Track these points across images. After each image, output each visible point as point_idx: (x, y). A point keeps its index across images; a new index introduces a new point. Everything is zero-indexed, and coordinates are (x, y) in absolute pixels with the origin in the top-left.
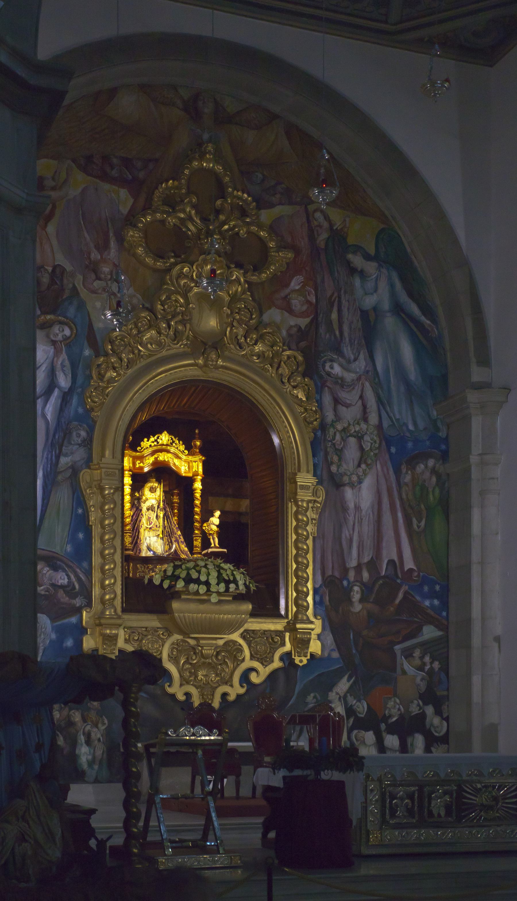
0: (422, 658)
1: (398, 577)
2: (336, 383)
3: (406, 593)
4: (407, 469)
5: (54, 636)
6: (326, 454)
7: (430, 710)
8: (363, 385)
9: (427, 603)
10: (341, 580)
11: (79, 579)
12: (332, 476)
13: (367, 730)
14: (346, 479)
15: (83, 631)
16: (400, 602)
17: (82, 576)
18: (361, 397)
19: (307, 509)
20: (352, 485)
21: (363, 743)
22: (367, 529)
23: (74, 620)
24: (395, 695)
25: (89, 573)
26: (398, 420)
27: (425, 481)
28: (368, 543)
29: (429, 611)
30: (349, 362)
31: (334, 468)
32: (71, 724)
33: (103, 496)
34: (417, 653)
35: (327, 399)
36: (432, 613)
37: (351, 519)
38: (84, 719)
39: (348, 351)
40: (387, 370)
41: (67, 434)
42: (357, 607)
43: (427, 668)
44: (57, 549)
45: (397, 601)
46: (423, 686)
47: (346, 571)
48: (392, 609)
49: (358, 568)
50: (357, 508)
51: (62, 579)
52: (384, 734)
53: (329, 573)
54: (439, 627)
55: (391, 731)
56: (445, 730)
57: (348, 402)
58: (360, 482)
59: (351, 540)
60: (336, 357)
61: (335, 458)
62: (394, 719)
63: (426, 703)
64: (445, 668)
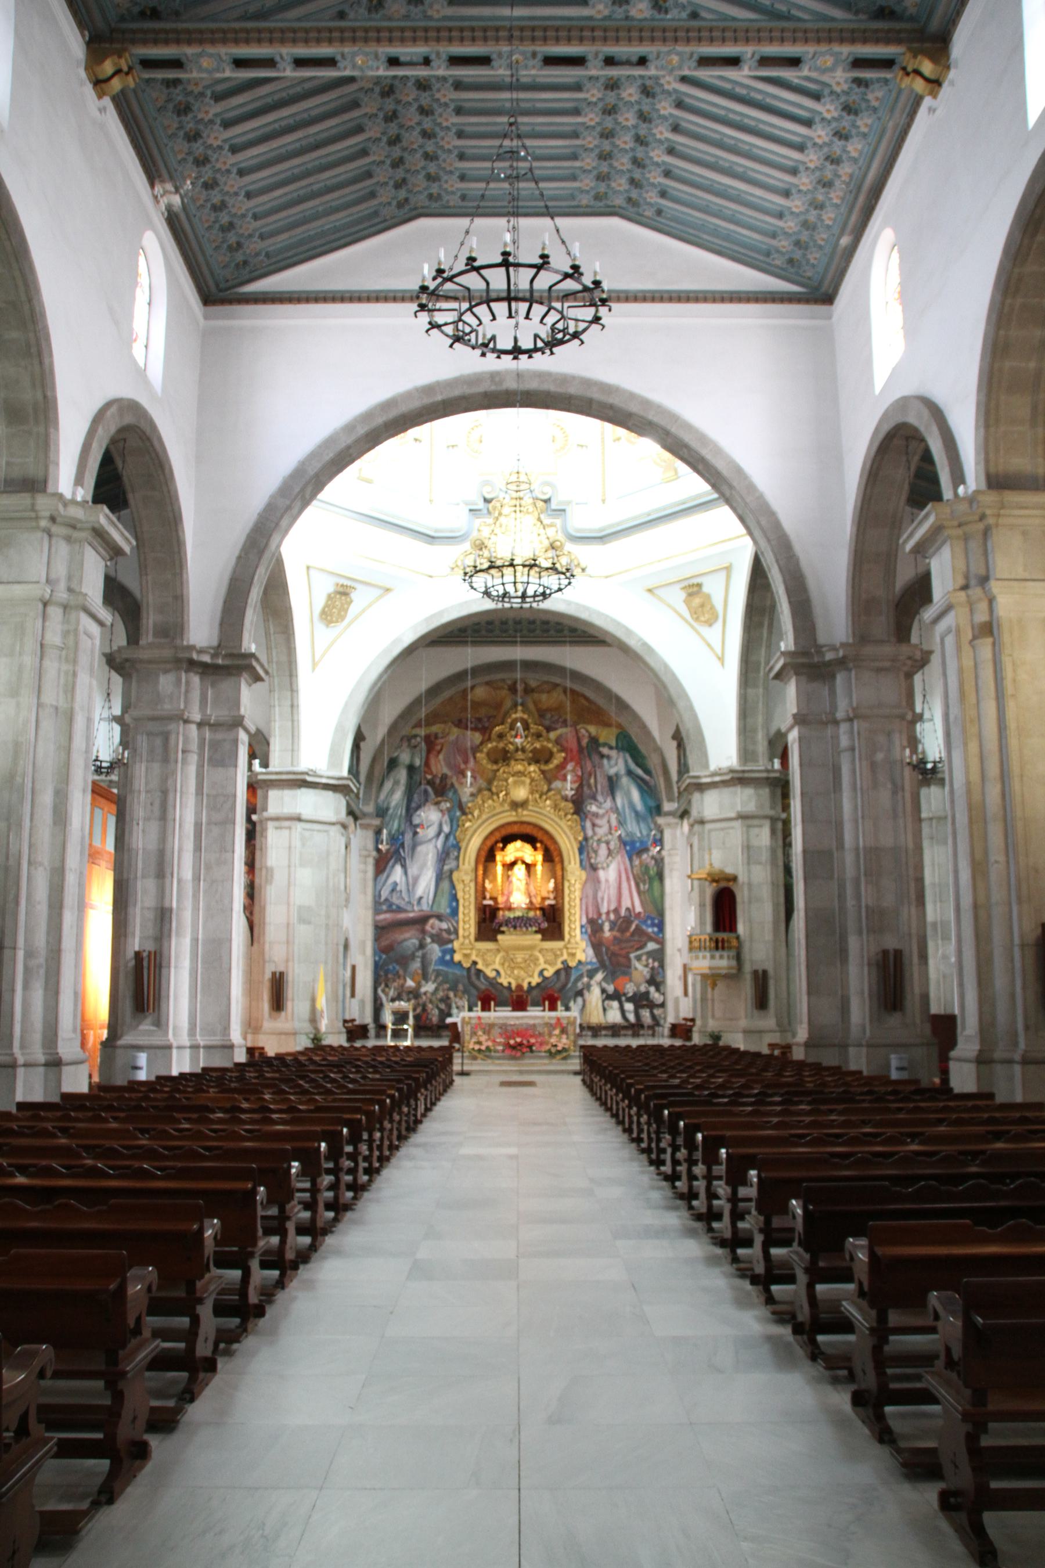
0: (647, 960)
3: (637, 926)
5: (440, 954)
6: (588, 853)
7: (652, 989)
9: (650, 930)
14: (600, 866)
15: (454, 951)
18: (609, 822)
20: (603, 869)
21: (611, 1007)
22: (613, 892)
23: (450, 946)
24: (631, 980)
25: (457, 922)
28: (614, 899)
31: (593, 861)
32: (448, 998)
34: (644, 958)
35: (588, 824)
37: (603, 885)
38: (455, 996)
39: (600, 798)
42: (607, 934)
46: (648, 976)
47: (600, 915)
48: (628, 934)
49: (608, 913)
50: (607, 881)
53: (590, 916)
55: (629, 1000)
58: (608, 866)
59: (603, 899)
61: (593, 855)
64: (662, 966)
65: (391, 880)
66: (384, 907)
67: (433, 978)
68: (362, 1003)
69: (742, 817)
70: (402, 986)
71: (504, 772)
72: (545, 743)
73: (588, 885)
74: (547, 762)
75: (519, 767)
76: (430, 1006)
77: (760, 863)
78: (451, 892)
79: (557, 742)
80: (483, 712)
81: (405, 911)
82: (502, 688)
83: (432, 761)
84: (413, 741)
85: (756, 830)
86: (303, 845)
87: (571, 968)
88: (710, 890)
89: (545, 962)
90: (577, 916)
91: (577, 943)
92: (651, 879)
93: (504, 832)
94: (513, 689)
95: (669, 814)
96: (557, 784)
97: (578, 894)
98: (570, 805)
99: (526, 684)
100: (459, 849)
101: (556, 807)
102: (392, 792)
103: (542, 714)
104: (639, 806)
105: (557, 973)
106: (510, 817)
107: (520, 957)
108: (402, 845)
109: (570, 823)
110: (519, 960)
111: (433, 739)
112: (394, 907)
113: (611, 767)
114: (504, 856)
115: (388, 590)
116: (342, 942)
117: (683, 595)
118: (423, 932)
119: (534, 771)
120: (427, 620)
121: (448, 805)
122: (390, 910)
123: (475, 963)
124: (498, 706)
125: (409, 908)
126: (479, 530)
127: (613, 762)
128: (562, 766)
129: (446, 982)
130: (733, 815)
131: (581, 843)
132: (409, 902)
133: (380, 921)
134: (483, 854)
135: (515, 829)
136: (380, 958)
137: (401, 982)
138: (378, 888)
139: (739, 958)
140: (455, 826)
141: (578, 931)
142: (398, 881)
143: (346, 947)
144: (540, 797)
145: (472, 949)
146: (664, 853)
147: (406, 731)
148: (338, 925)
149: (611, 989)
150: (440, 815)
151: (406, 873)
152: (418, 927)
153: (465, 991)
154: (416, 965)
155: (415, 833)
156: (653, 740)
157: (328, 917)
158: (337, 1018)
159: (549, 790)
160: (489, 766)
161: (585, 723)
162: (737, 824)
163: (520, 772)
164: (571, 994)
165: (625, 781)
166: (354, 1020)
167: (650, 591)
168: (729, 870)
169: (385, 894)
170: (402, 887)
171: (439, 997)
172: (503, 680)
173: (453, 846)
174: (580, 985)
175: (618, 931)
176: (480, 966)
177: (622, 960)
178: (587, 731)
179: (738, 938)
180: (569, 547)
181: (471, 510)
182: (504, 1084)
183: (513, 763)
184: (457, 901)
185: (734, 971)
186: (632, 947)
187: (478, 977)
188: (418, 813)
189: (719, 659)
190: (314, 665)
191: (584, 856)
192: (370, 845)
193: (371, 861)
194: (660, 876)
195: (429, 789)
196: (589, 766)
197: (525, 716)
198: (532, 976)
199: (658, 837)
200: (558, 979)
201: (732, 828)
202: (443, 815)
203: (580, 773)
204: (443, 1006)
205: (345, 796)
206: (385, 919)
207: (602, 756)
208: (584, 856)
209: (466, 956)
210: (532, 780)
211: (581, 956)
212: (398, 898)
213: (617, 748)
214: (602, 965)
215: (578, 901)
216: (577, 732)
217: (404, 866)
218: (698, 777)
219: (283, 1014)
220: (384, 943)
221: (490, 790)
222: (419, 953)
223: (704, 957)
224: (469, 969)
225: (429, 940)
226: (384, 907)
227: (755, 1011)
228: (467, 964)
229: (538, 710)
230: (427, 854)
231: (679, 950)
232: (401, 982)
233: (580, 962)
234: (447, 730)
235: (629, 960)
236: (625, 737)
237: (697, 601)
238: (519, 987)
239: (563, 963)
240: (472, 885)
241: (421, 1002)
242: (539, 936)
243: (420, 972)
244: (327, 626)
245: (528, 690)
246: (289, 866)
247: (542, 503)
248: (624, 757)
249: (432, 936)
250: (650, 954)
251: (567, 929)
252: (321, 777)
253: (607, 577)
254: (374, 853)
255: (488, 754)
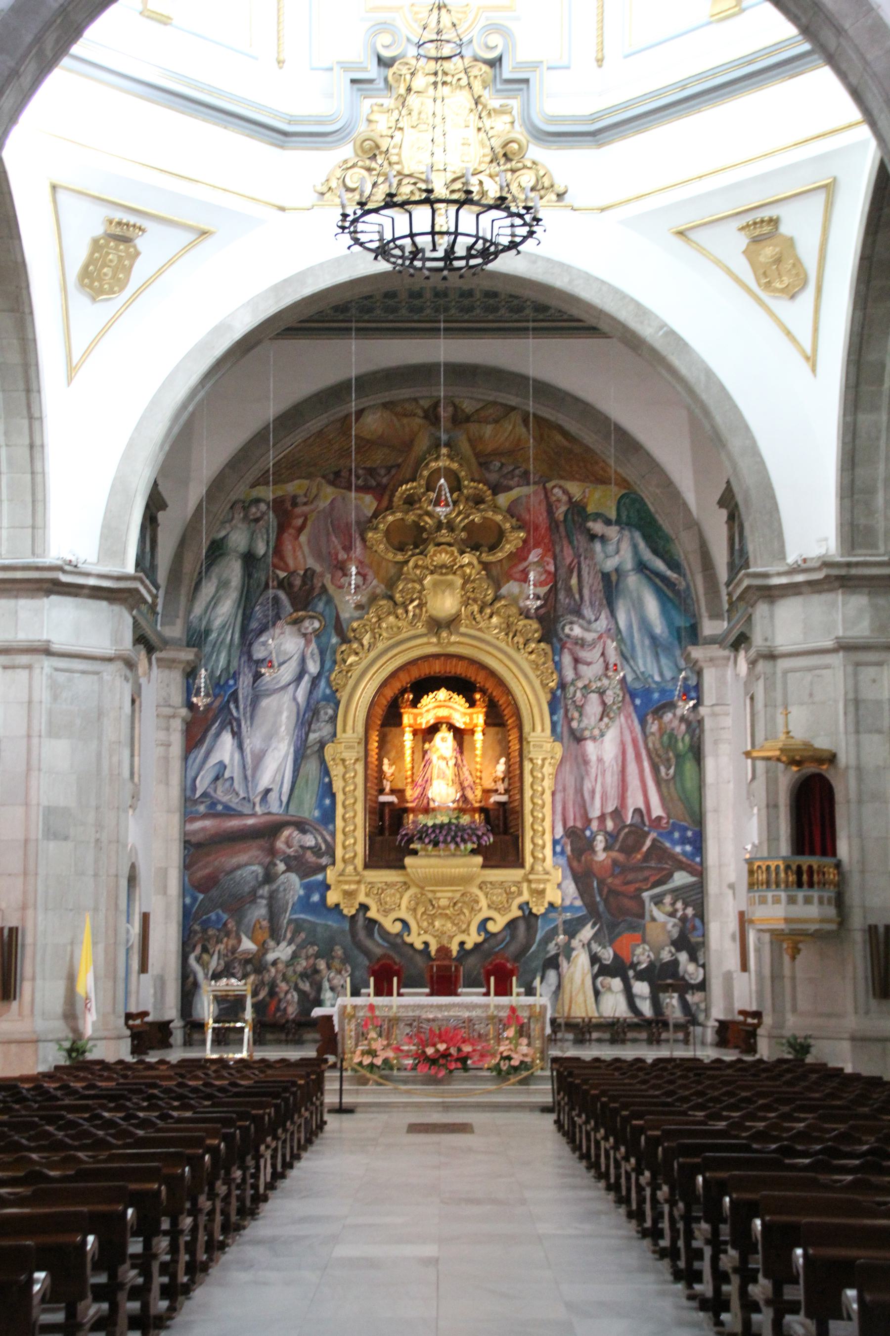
0: (673, 904)
1: (645, 825)
2: (576, 644)
3: (654, 840)
4: (654, 720)
5: (302, 892)
7: (683, 957)
8: (605, 643)
9: (678, 849)
10: (583, 831)
11: (325, 841)
12: (572, 732)
13: (613, 976)
14: (587, 734)
15: (328, 887)
16: (649, 849)
17: (329, 838)
18: (603, 654)
19: (543, 766)
20: (594, 739)
21: (609, 989)
22: (611, 780)
23: (320, 877)
24: (644, 941)
25: (333, 834)
26: (643, 673)
27: (673, 729)
29: (681, 858)
30: (589, 622)
31: (574, 724)
32: (316, 971)
33: (345, 767)
34: (668, 900)
35: (567, 660)
36: (684, 859)
37: (593, 771)
38: (329, 967)
39: (588, 612)
40: (630, 627)
41: (316, 713)
42: (601, 856)
43: (679, 914)
44: (306, 815)
45: (645, 848)
46: (675, 934)
47: (588, 821)
48: (639, 856)
49: (602, 818)
50: (600, 760)
51: (309, 840)
52: (632, 981)
53: (571, 823)
54: (692, 873)
55: (641, 976)
56: (701, 977)
57: (589, 660)
58: (602, 735)
59: (593, 792)
60: (575, 619)
61: (576, 715)
62: (644, 966)
63: (679, 950)
64: (701, 915)
65: (213, 760)
66: (202, 808)
67: (289, 935)
68: (160, 982)
69: (844, 647)
70: (234, 950)
71: (416, 566)
72: (490, 514)
73: (567, 767)
74: (492, 548)
75: (444, 558)
76: (283, 986)
77: (879, 731)
78: (321, 780)
79: (511, 512)
80: (378, 458)
81: (240, 815)
82: (415, 415)
83: (288, 547)
84: (254, 510)
85: (871, 671)
86: (55, 698)
87: (536, 916)
88: (786, 779)
89: (489, 907)
90: (547, 824)
91: (547, 873)
92: (678, 756)
93: (416, 673)
94: (432, 416)
95: (713, 640)
96: (511, 588)
97: (548, 784)
98: (535, 625)
99: (454, 406)
100: (337, 704)
101: (508, 628)
102: (215, 601)
103: (483, 461)
104: (659, 627)
105: (512, 924)
106: (428, 646)
107: (444, 897)
108: (234, 697)
109: (533, 656)
110: (443, 902)
111: (288, 505)
112: (220, 807)
113: (607, 557)
114: (416, 716)
115: (204, 233)
116: (125, 871)
117: (742, 241)
118: (272, 852)
119: (469, 564)
120: (276, 289)
121: (317, 624)
122: (212, 814)
123: (364, 908)
124: (408, 445)
125: (247, 811)
126: (370, 121)
127: (611, 548)
128: (520, 555)
129: (313, 944)
130: (829, 644)
131: (553, 692)
132: (246, 799)
133: (195, 832)
134: (380, 712)
135: (437, 668)
136: (195, 899)
137: (232, 942)
138: (191, 773)
139: (840, 902)
140: (328, 665)
141: (548, 851)
142: (227, 761)
143: (132, 880)
144: (481, 611)
145: (359, 882)
146: (703, 710)
147: (241, 491)
148: (118, 841)
149: (607, 955)
150: (302, 642)
151: (240, 747)
152: (262, 842)
153: (347, 959)
154: (259, 912)
155: (258, 676)
156: (685, 504)
157: (99, 826)
158: (114, 1012)
159: (497, 598)
160: (390, 556)
161: (562, 478)
162: (837, 660)
163: (443, 566)
164: (538, 963)
165: (633, 581)
166: (145, 1014)
167: (681, 233)
168: (822, 743)
169: (202, 785)
170: (233, 771)
171: (299, 969)
172: (416, 400)
173: (326, 698)
174: (552, 949)
175: (621, 850)
176: (372, 914)
177: (628, 903)
178: (565, 492)
179: (838, 865)
180: (535, 152)
181: (353, 81)
182: (414, 1128)
183: (432, 549)
184: (333, 796)
185: (833, 927)
186: (646, 879)
187: (370, 934)
188: (262, 639)
189: (807, 359)
190: (72, 371)
191: (560, 715)
192: (177, 697)
193: (177, 725)
194: (697, 753)
195: (282, 595)
196: (568, 555)
197: (455, 466)
198: (466, 931)
199: (693, 682)
200: (513, 937)
201: (827, 667)
202: (308, 643)
203: (552, 568)
204: (306, 986)
205: (131, 609)
206: (203, 829)
207: (593, 537)
208: (560, 715)
209: (349, 894)
210: (467, 580)
211: (553, 895)
212: (226, 792)
213: (618, 522)
214: (592, 913)
215: (548, 797)
216: (547, 493)
217: (237, 735)
218: (766, 575)
219: (15, 1005)
220: (200, 874)
221: (391, 598)
222: (265, 891)
223: (776, 901)
224: (353, 917)
225: (281, 867)
226: (202, 808)
227: (873, 1003)
228: (349, 911)
229: (477, 455)
230: (279, 712)
231: (731, 886)
232: (232, 942)
233: (551, 905)
234: (314, 491)
235: (642, 903)
236: (634, 501)
237: (768, 252)
238: (444, 951)
239: (520, 907)
240: (360, 767)
241: (267, 978)
242: (479, 860)
243: (265, 923)
244: (94, 299)
245: (459, 419)
246: (29, 736)
247: (485, 68)
248: (632, 539)
249: (287, 860)
250: (677, 893)
251: (528, 847)
252: (87, 575)
253: (603, 210)
254: (184, 712)
255: (387, 533)
